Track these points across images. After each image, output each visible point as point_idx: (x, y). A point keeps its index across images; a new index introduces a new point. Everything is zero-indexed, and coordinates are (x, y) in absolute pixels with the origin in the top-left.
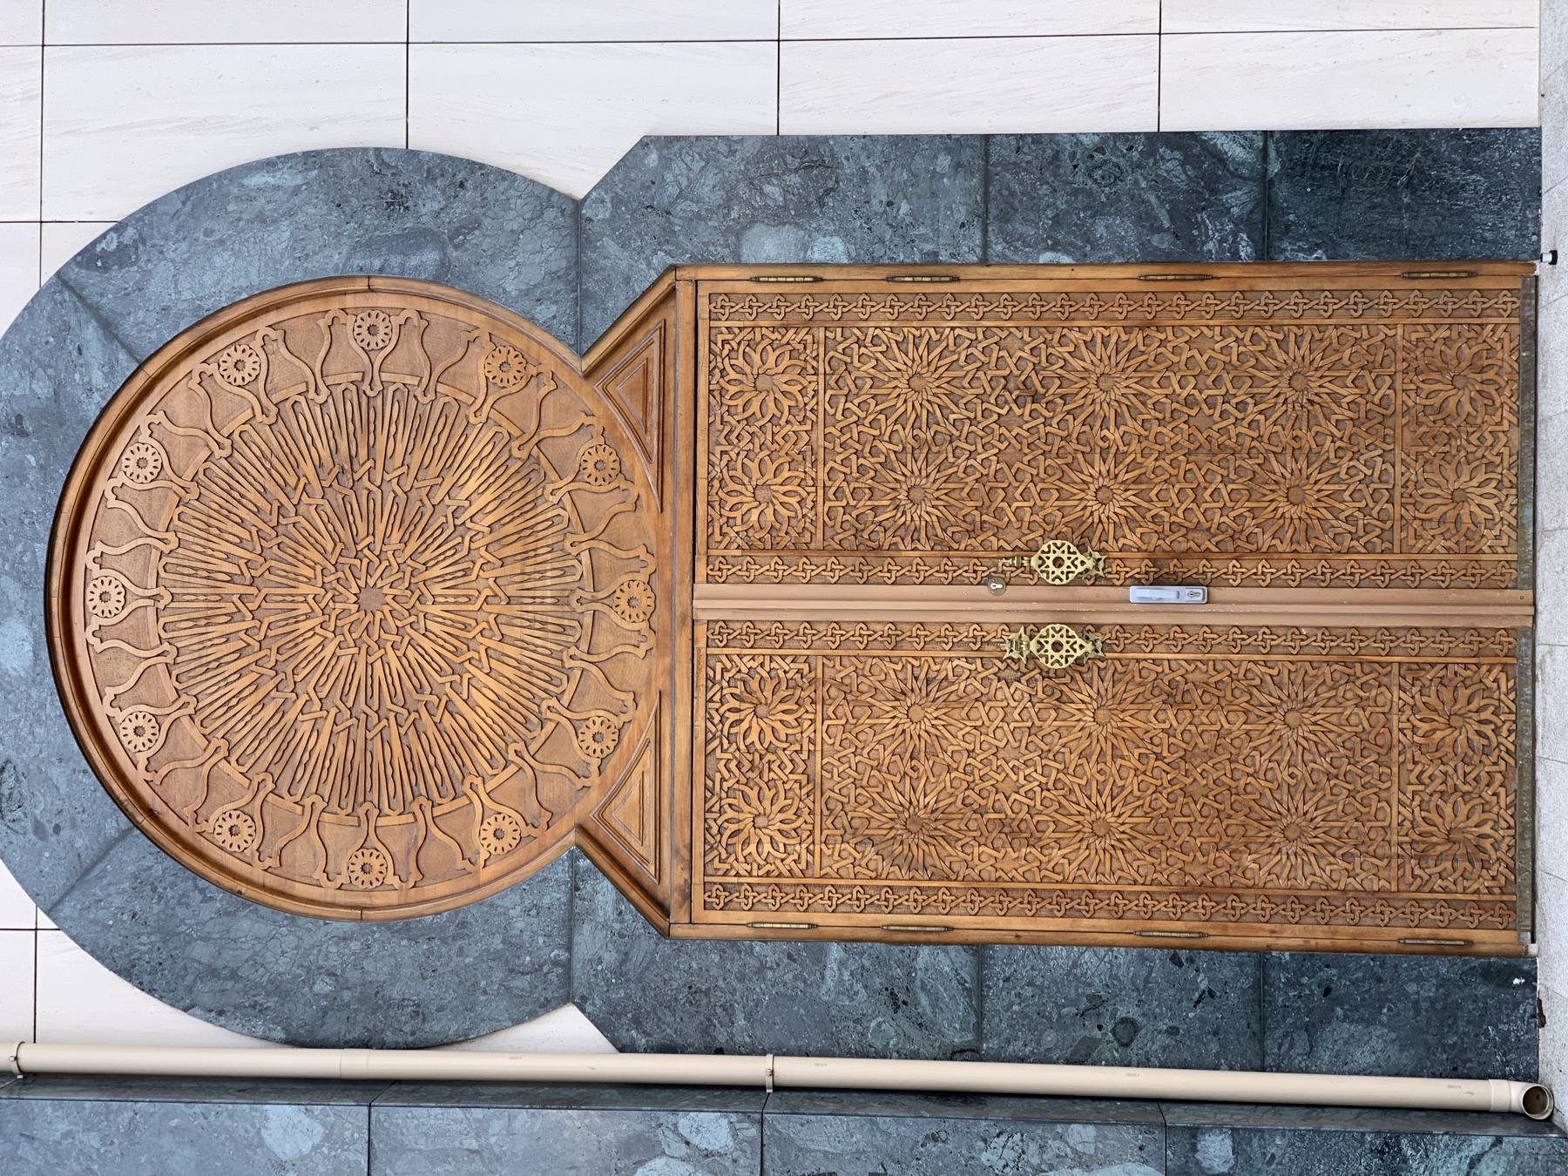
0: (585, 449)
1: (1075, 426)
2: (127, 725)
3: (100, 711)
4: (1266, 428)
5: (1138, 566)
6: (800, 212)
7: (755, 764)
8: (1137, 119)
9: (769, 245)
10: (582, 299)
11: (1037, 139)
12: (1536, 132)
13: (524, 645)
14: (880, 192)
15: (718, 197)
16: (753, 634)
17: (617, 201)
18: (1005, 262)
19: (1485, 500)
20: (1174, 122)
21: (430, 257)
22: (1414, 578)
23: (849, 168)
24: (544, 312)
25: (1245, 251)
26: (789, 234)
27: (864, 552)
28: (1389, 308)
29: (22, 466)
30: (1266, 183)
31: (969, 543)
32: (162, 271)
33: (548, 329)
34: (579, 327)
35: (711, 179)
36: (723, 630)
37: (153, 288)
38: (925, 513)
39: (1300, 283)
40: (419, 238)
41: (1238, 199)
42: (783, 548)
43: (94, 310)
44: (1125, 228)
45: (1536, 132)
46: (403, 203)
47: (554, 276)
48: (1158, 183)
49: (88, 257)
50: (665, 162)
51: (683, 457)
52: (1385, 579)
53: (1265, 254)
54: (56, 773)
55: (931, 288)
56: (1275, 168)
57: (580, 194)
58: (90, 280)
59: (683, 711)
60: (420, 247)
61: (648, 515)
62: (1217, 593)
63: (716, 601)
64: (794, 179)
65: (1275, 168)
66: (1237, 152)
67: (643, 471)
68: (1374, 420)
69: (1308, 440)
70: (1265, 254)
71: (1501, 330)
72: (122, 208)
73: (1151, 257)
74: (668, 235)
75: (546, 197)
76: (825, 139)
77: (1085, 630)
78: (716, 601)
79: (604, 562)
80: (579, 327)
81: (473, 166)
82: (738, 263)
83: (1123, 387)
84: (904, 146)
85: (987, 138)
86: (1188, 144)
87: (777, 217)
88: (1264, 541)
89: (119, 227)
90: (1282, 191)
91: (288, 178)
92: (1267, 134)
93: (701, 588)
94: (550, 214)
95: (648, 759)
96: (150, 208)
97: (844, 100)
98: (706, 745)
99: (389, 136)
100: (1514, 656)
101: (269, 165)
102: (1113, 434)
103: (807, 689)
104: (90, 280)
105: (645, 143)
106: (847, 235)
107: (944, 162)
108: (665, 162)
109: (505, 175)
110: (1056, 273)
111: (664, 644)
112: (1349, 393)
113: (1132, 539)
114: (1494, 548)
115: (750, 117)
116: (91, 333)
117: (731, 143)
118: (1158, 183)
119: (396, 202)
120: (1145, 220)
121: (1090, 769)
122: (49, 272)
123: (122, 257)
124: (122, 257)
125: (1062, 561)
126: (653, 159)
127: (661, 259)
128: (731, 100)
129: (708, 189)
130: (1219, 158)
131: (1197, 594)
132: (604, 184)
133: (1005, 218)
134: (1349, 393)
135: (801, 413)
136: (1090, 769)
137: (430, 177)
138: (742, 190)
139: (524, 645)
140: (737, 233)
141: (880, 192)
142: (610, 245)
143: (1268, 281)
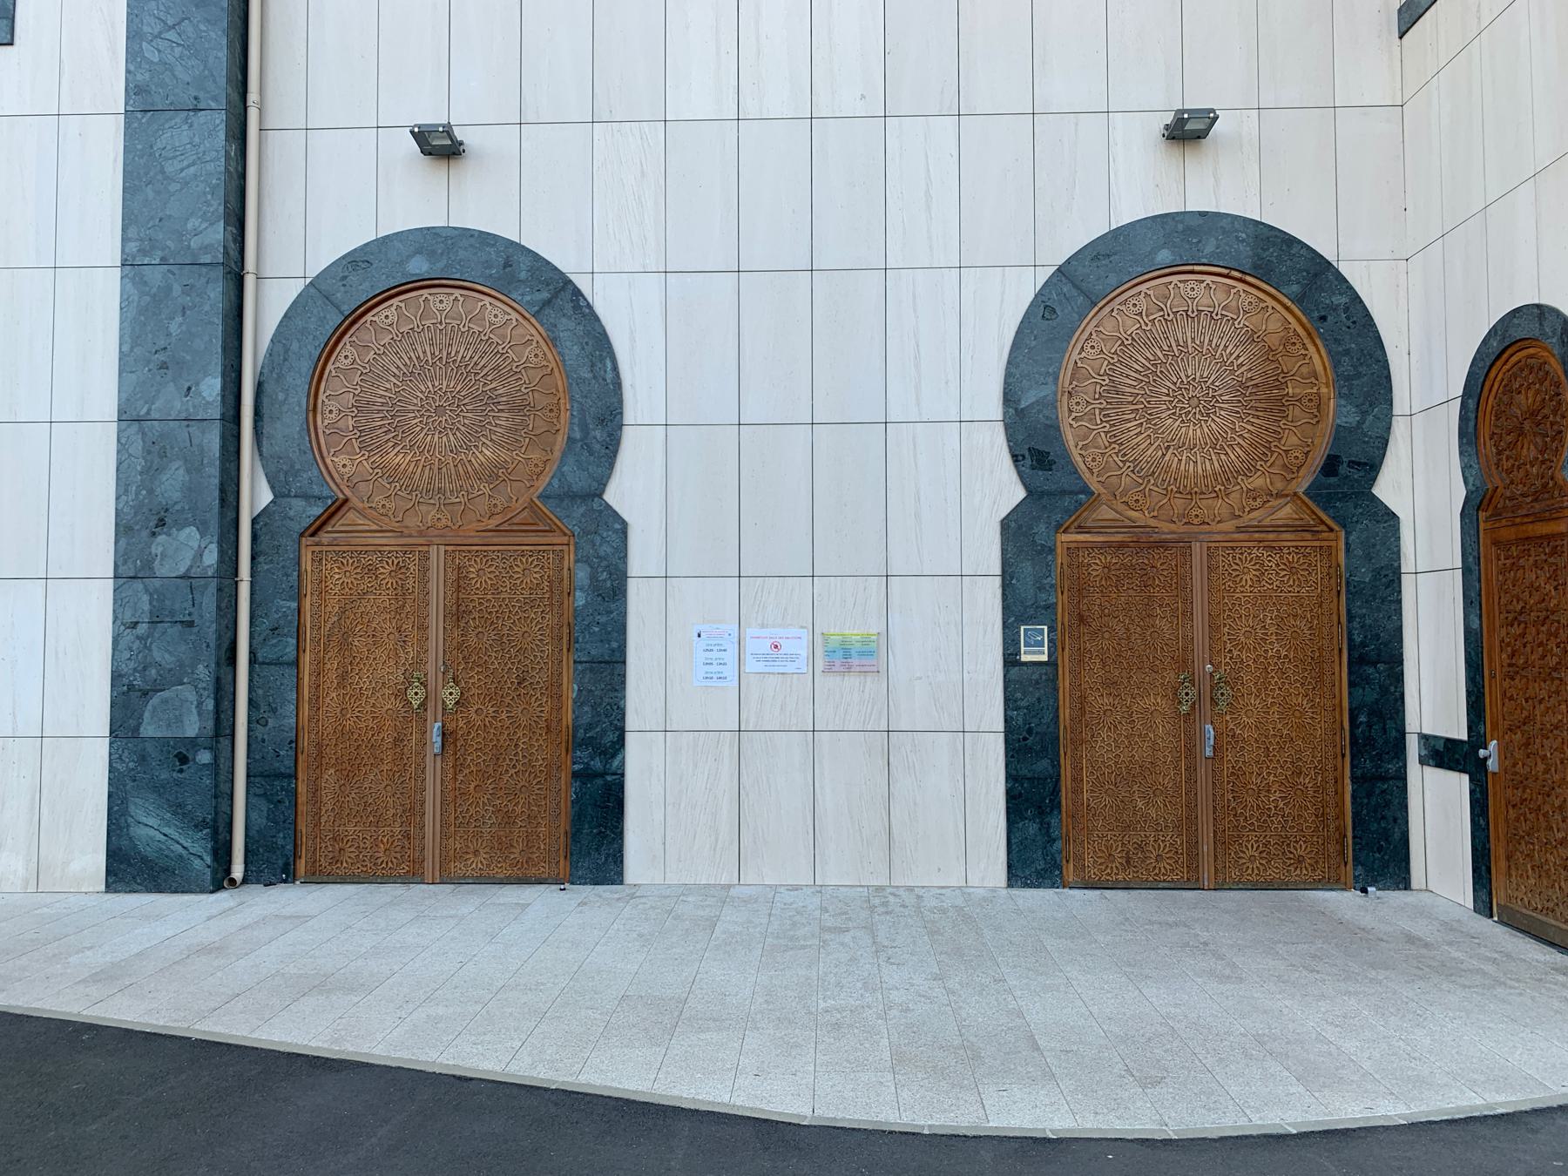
0: (501, 501)
1: (507, 700)
2: (387, 313)
3: (395, 301)
4: (506, 777)
5: (451, 726)
6: (595, 586)
7: (371, 570)
8: (632, 722)
9: (582, 575)
10: (560, 498)
11: (624, 682)
12: (621, 883)
13: (421, 476)
14: (603, 619)
15: (602, 554)
16: (424, 570)
17: (600, 512)
18: (575, 670)
19: (476, 864)
20: (630, 738)
21: (578, 435)
22: (445, 836)
23: (613, 606)
24: (556, 483)
25: (576, 767)
26: (586, 582)
27: (457, 614)
28: (554, 821)
29: (490, 267)
30: (602, 775)
31: (461, 658)
32: (572, 325)
33: (550, 484)
34: (548, 497)
35: (609, 550)
36: (425, 557)
37: (564, 320)
38: (472, 639)
39: (565, 790)
40: (585, 428)
41: (597, 764)
42: (459, 583)
43: (555, 295)
44: (586, 719)
45: (621, 883)
46: (600, 425)
47: (570, 486)
48: (604, 731)
49: (577, 293)
50: (616, 531)
51: (495, 540)
52: (445, 824)
53: (575, 775)
54: (366, 285)
55: (565, 641)
56: (609, 778)
57: (606, 497)
58: (567, 295)
59: (393, 541)
60: (582, 431)
61: (475, 525)
62: (439, 759)
63: (436, 555)
64: (609, 584)
65: (609, 778)
66: (616, 763)
67: (492, 524)
68: (508, 819)
69: (501, 793)
70: (575, 775)
71: (544, 870)
72: (600, 309)
73: (576, 728)
74: (586, 533)
75: (603, 484)
76: (625, 596)
77: (423, 705)
78: (436, 555)
79: (456, 508)
80: (548, 497)
81: (615, 453)
82: (576, 561)
83: (524, 720)
84: (622, 629)
85: (624, 662)
86: (620, 743)
87: (593, 578)
88: (460, 777)
89: (589, 306)
90: (599, 781)
91: (609, 376)
92: (623, 775)
93: (442, 548)
94: (595, 484)
95: (375, 527)
96: (597, 319)
97: (641, 602)
98: (378, 550)
99: (629, 416)
100: (412, 874)
101: (615, 368)
102: (504, 716)
103: (401, 593)
104: (567, 295)
105: (624, 524)
106: (585, 606)
107: (615, 645)
108: (616, 531)
109: (612, 466)
110: (570, 691)
111: (421, 534)
112: (518, 810)
113: (461, 724)
114: (456, 868)
115: (635, 565)
116: (545, 295)
117: (624, 558)
118: (604, 731)
119: (602, 421)
120: (590, 727)
121: (368, 708)
122: (572, 277)
123: (577, 307)
124: (577, 307)
125: (450, 695)
126: (617, 526)
127: (577, 530)
128: (642, 557)
129: (605, 549)
130: (613, 756)
131: (437, 748)
132: (608, 506)
133: (591, 670)
134: (518, 810)
135: (514, 587)
136: (368, 708)
137: (610, 435)
138: (604, 563)
139: (421, 476)
140: (587, 561)
141: (603, 619)
142: (582, 510)
143: (565, 777)
